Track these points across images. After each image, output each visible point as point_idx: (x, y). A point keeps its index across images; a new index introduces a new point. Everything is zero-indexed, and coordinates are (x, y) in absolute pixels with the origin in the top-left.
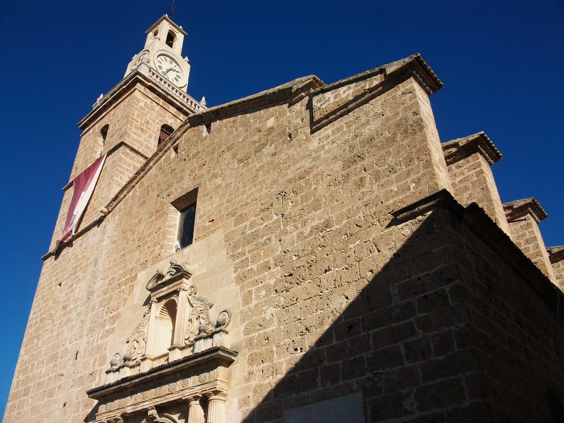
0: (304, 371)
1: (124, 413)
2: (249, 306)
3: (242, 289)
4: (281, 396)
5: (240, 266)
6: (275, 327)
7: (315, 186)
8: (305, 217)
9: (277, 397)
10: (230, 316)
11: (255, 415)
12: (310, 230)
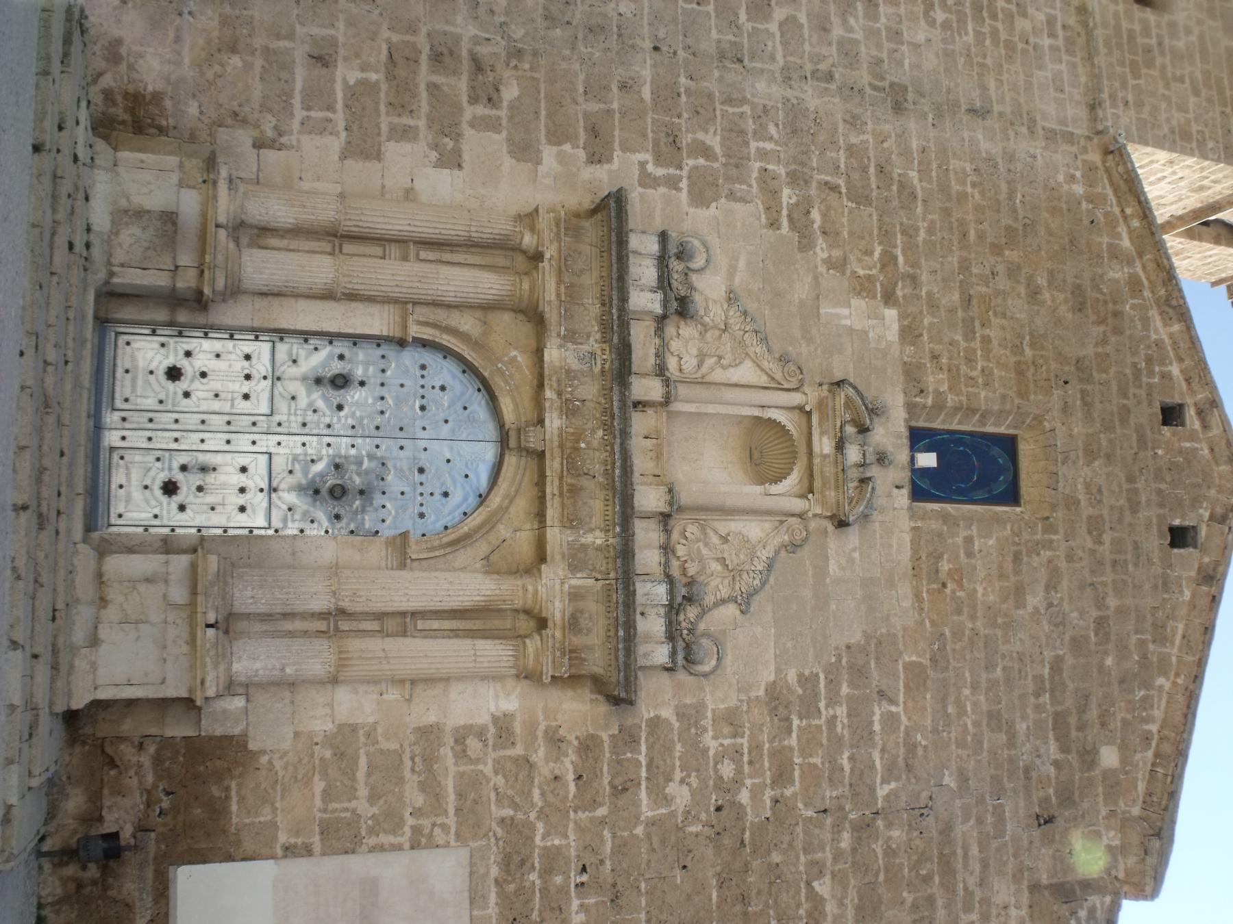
0: (538, 895)
4: (499, 836)
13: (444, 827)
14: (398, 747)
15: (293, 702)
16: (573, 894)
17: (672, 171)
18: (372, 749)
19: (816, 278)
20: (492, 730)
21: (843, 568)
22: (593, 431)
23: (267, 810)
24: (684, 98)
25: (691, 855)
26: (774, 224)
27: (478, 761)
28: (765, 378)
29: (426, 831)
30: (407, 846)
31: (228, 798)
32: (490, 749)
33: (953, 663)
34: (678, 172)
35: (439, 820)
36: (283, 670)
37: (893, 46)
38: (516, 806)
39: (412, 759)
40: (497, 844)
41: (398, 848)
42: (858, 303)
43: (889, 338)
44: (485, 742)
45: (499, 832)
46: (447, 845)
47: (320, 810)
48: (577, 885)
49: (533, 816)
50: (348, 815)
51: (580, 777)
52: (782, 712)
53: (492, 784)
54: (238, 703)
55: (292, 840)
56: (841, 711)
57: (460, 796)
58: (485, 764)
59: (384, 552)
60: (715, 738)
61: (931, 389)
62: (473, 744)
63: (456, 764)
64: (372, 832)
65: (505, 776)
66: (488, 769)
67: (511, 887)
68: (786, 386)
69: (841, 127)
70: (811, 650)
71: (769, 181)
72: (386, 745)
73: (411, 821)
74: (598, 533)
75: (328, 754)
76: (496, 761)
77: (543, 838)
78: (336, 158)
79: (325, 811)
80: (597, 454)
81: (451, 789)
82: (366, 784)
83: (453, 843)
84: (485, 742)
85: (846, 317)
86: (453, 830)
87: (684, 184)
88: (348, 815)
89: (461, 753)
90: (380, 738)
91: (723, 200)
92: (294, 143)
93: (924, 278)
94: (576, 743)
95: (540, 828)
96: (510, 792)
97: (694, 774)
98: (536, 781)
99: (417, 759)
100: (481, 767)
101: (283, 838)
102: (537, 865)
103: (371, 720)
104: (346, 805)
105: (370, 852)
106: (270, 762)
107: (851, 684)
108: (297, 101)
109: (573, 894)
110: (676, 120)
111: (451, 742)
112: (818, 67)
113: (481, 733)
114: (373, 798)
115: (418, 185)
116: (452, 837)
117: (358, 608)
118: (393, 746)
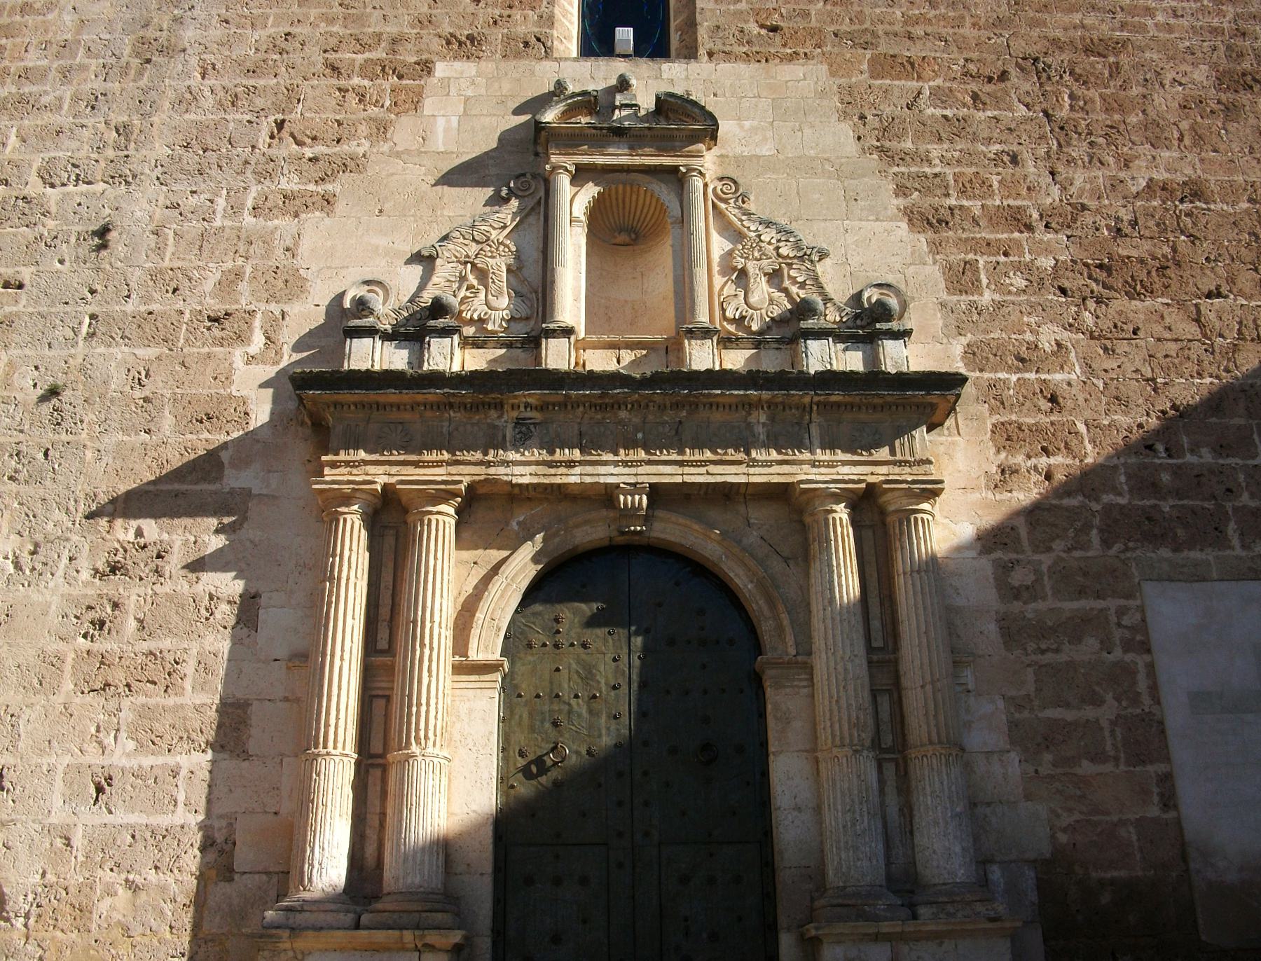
0: (1185, 502)
1: (486, 479)
2: (971, 298)
3: (935, 247)
5: (918, 187)
6: (1075, 377)
7: (1141, 90)
8: (1125, 149)
9: (1109, 548)
10: (904, 306)
11: (1046, 578)
12: (1145, 184)
13: (1121, 612)
14: (1030, 670)
15: (989, 804)
16: (1180, 461)
17: (257, 323)
18: (1036, 703)
19: (398, 155)
20: (998, 554)
21: (765, 139)
22: (621, 422)
23: (1123, 832)
24: (154, 307)
25: (1119, 324)
26: (328, 201)
27: (1037, 572)
28: (532, 219)
29: (1127, 634)
30: (1147, 658)
31: (1113, 882)
32: (1021, 557)
33: (867, 25)
34: (259, 315)
35: (1113, 619)
36: (958, 815)
37: (81, 51)
38: (1087, 527)
39: (1043, 652)
40: (1134, 549)
41: (1151, 667)
42: (428, 106)
43: (474, 73)
44: (1014, 563)
45: (1117, 547)
46: (1142, 609)
47: (1117, 766)
48: (1170, 456)
49: (1096, 507)
50: (1118, 731)
51: (1044, 449)
52: (944, 213)
53: (1064, 555)
54: (996, 873)
55: (1156, 799)
56: (935, 151)
57: (1081, 592)
58: (1040, 562)
59: (788, 690)
60: (981, 294)
61: (536, 30)
62: (1019, 577)
63: (1044, 598)
64: (1135, 700)
65: (1052, 540)
66: (1046, 560)
67: (1180, 532)
68: (542, 193)
69: (192, 116)
70: (866, 179)
71: (268, 204)
72: (1030, 688)
73: (1118, 654)
74: (752, 419)
75: (1048, 757)
76: (1036, 550)
77: (1120, 494)
78: (246, 764)
79: (1116, 759)
80: (651, 417)
81: (1075, 605)
82: (1079, 709)
83: (1138, 602)
84: (1014, 563)
85: (448, 122)
86: (1122, 602)
87: (275, 308)
88: (1118, 731)
89: (1030, 592)
90: (1023, 692)
91: (298, 262)
92: (224, 823)
93: (391, 29)
94: (1003, 455)
95: (1107, 498)
96: (1071, 533)
97: (1025, 319)
98: (1054, 502)
99: (1043, 646)
100: (1044, 568)
101: (1154, 811)
102: (1152, 502)
103: (1001, 704)
104: (1107, 734)
105: (1159, 703)
106: (1064, 830)
107: (900, 137)
108: (163, 821)
109: (1180, 461)
110: (187, 316)
111: (1017, 606)
112: (111, 142)
113: (1004, 569)
114: (1097, 702)
115: (281, 652)
116: (1131, 603)
117: (870, 722)
118: (1030, 675)
